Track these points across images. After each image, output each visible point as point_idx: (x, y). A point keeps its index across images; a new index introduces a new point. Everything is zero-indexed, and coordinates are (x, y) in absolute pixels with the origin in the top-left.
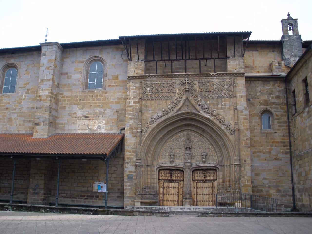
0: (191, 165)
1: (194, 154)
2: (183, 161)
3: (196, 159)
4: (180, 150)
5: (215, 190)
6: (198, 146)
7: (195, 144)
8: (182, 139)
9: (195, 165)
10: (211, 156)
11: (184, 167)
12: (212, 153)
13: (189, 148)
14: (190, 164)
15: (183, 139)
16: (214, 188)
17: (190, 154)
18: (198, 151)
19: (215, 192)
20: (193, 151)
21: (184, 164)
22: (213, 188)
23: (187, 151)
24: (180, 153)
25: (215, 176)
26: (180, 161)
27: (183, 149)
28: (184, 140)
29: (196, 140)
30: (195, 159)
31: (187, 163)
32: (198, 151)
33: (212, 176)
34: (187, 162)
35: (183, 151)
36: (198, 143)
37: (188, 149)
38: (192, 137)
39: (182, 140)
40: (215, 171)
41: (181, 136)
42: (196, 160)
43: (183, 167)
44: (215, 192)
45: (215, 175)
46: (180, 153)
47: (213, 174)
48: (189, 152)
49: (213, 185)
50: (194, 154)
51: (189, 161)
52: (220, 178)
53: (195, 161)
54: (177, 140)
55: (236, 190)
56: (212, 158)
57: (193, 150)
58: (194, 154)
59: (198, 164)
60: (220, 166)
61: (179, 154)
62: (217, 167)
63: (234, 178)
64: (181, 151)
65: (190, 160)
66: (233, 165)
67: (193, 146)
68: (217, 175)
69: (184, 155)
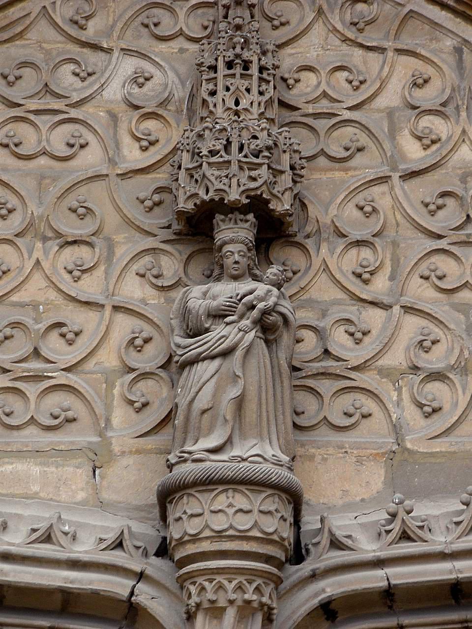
0: (298, 555)
1: (339, 340)
2: (133, 478)
3: (397, 429)
4: (81, 271)
6: (424, 189)
7: (367, 165)
8: (129, 66)
9: (368, 547)
11: (145, 595)
13: (257, 205)
14: (266, 518)
15: (140, 80)
17: (269, 327)
18: (421, 292)
20: (323, 290)
21: (145, 530)
23: (216, 272)
24: (77, 318)
26: (74, 479)
27: (127, 246)
28: (170, 73)
29: (390, 98)
30: (375, 433)
31: (209, 483)
32: (421, 292)
34: (219, 464)
35: (134, 290)
36: (428, 141)
37: (235, 236)
38: (316, 46)
39: (114, 91)
41: (92, 31)
42: (398, 460)
43: (119, 586)
46: (77, 318)
48: (260, 291)
50: (358, 336)
51: (259, 453)
53: (375, 477)
54: (30, 81)
57: (321, 281)
58: (358, 336)
59: (439, 541)
61: (53, 345)
64: (90, 287)
65: (271, 451)
67: (331, 199)
69: (150, 358)
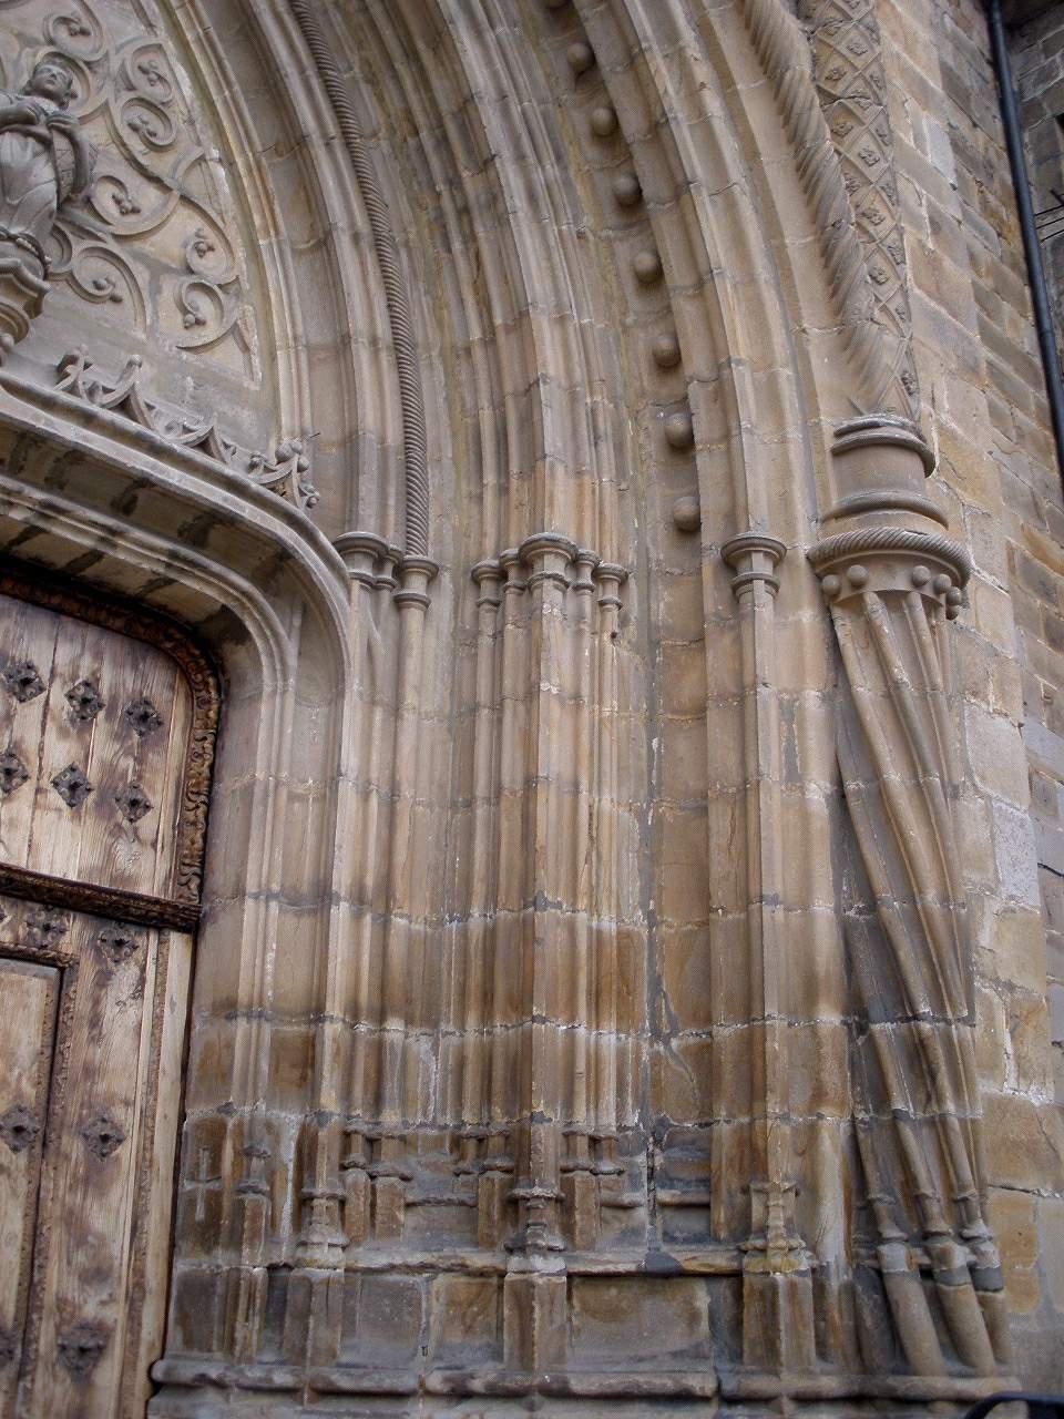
5: (121, 1194)
10: (158, 269)
12: (185, 224)
16: (106, 1141)
19: (97, 1274)
22: (75, 1148)
25: (158, 820)
33: (74, 789)
40: (158, 685)
44: (97, 1274)
45: (161, 795)
47: (101, 727)
49: (78, 1048)
52: (342, 879)
55: (960, 1256)
56: (171, 320)
60: (347, 547)
62: (276, 569)
63: (823, 907)
66: (800, 583)
68: (201, 793)
